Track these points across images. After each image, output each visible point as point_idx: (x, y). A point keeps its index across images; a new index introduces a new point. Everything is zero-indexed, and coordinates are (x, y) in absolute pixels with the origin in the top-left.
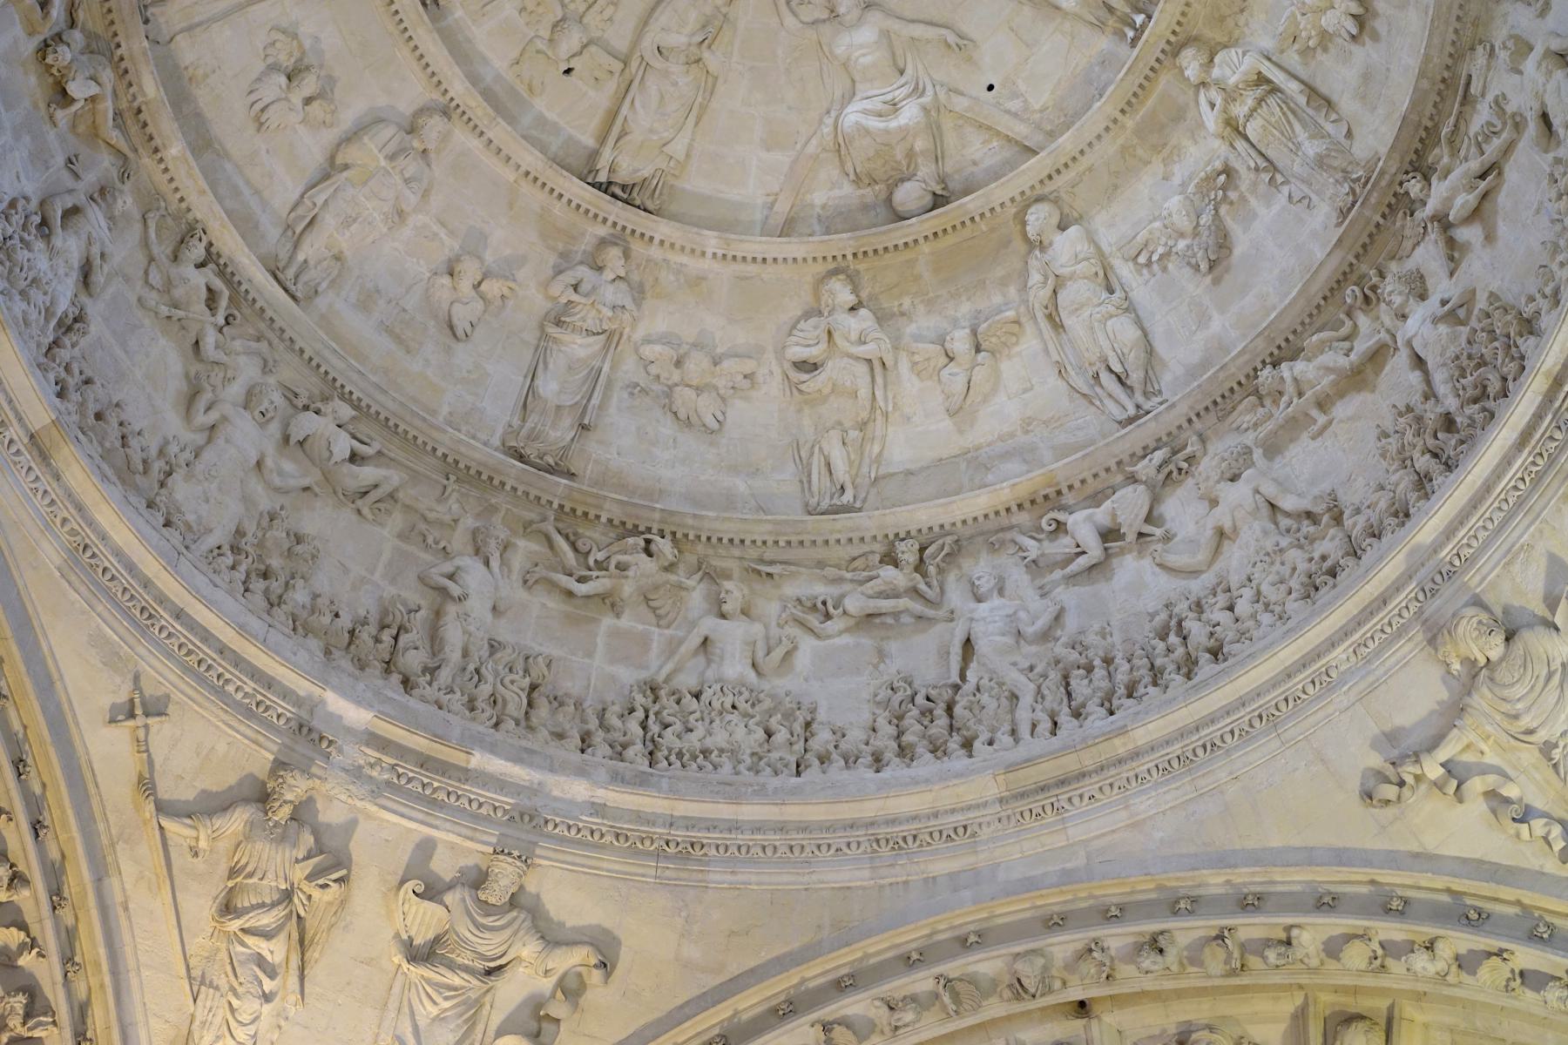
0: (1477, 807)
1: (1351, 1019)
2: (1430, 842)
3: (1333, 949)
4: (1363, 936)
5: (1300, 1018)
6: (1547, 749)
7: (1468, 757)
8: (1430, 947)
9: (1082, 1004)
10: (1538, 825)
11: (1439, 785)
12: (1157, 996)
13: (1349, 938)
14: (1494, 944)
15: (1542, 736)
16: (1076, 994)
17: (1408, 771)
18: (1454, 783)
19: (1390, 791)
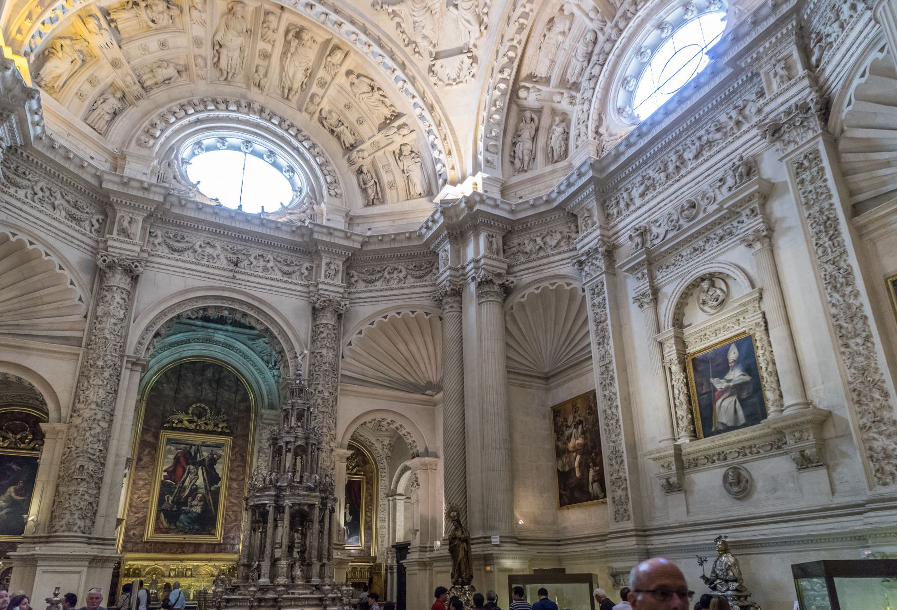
0: (394, 23)
1: (339, 48)
2: (381, 24)
3: (349, 33)
4: (357, 35)
5: (328, 41)
6: (415, 22)
7: (398, 12)
8: (369, 46)
9: (282, 7)
10: (404, 36)
11: (389, 14)
12: (300, 16)
13: (354, 33)
14: (383, 54)
15: (416, 19)
16: (284, 5)
17: (385, 6)
18: (392, 16)
19: (379, 8)
